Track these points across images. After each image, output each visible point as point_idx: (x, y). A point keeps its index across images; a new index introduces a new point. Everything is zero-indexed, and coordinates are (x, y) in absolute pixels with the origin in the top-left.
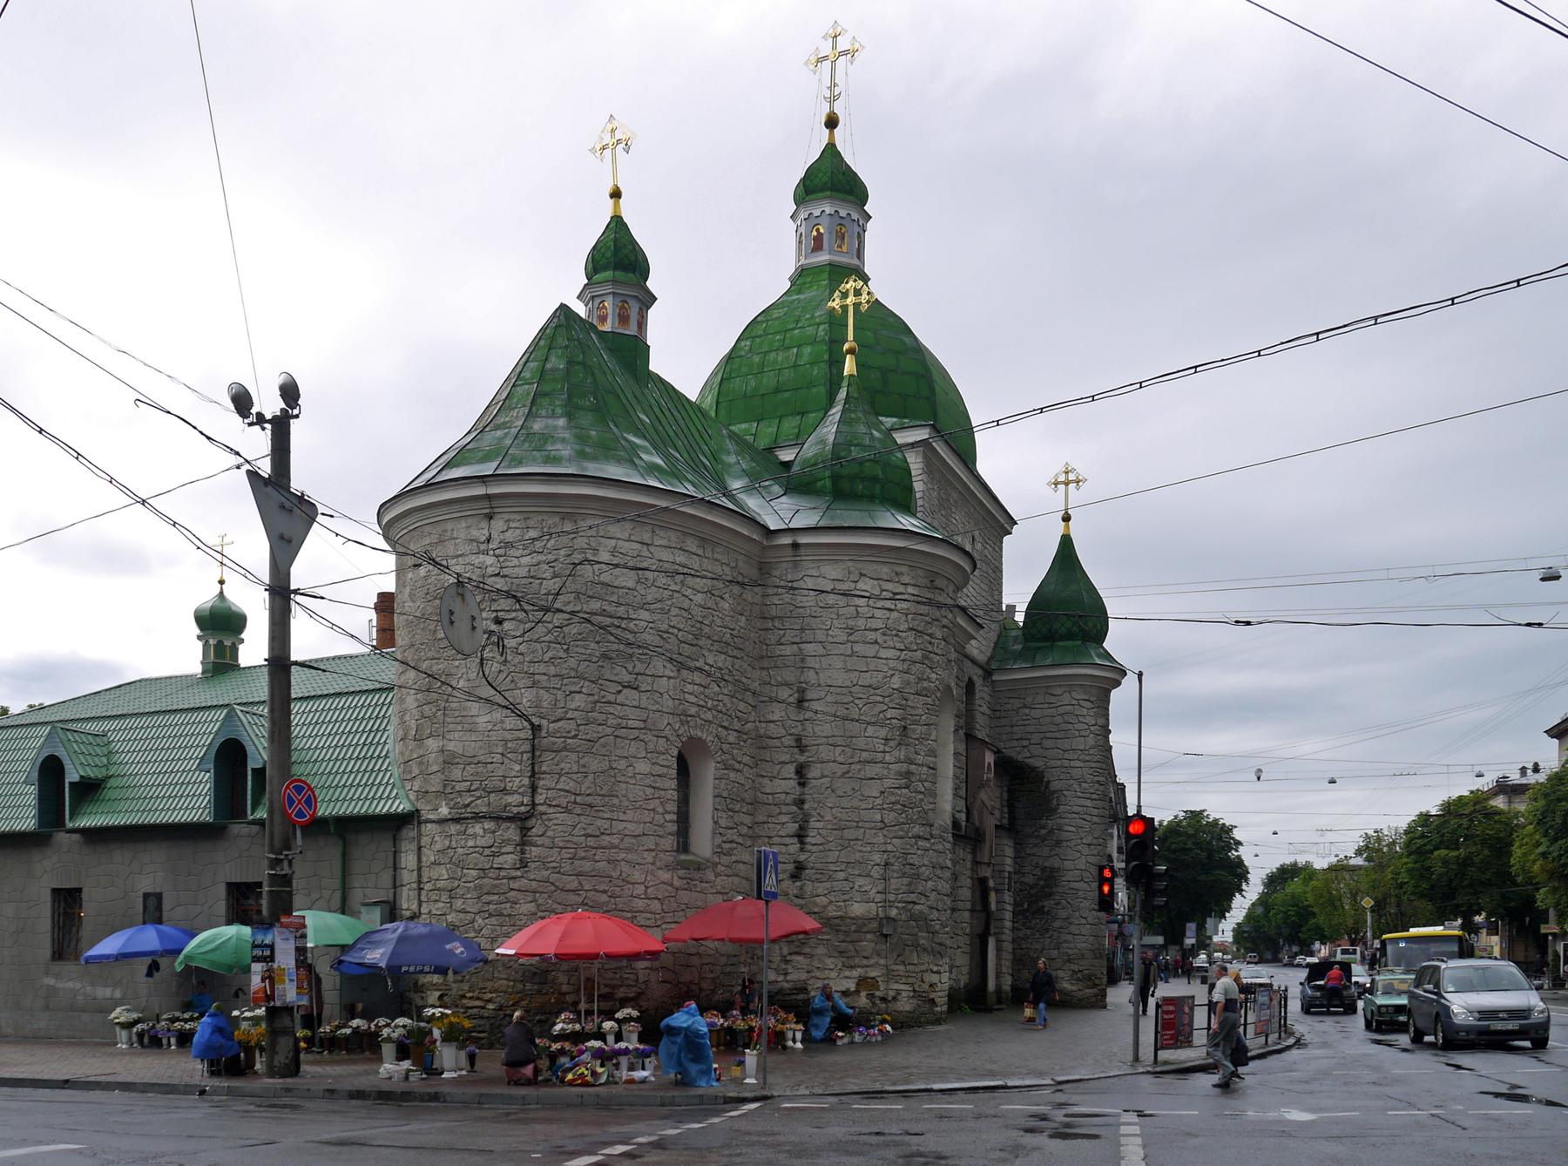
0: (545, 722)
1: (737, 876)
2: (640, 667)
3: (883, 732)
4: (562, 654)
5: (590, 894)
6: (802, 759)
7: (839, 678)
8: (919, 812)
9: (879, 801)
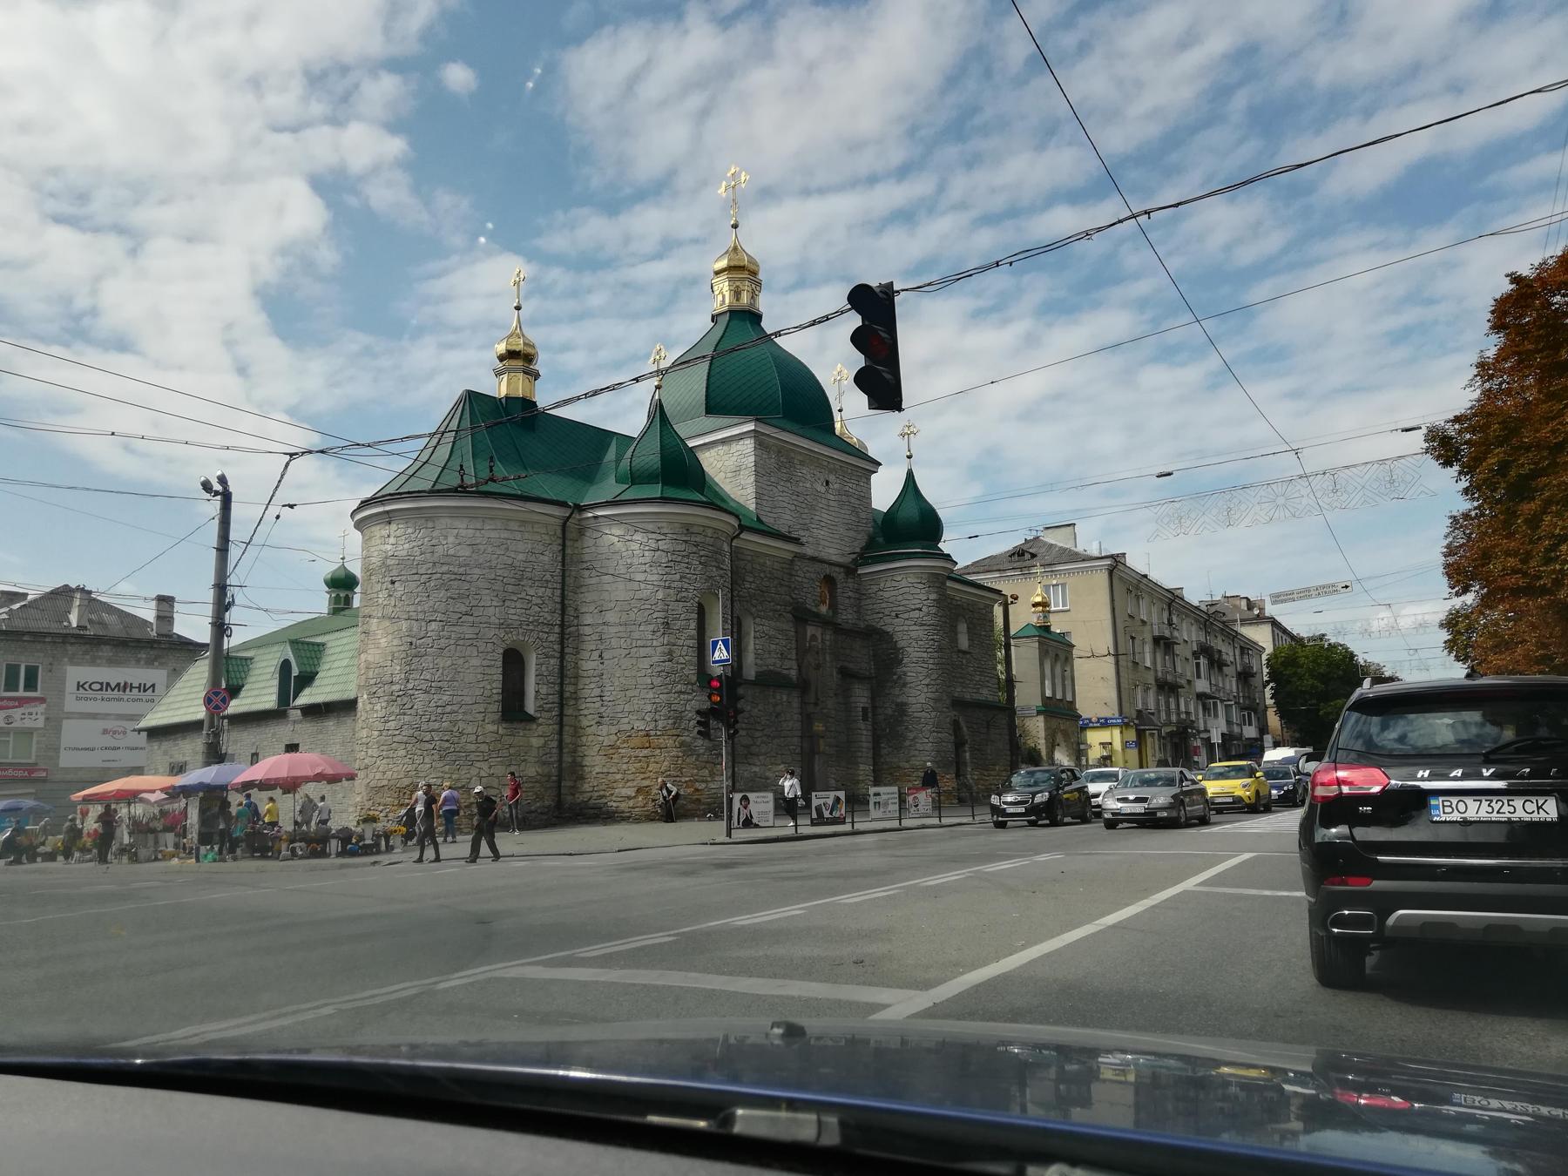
0: (414, 640)
2: (474, 603)
3: (651, 628)
4: (425, 599)
5: (438, 743)
6: (602, 647)
7: (622, 595)
9: (650, 671)
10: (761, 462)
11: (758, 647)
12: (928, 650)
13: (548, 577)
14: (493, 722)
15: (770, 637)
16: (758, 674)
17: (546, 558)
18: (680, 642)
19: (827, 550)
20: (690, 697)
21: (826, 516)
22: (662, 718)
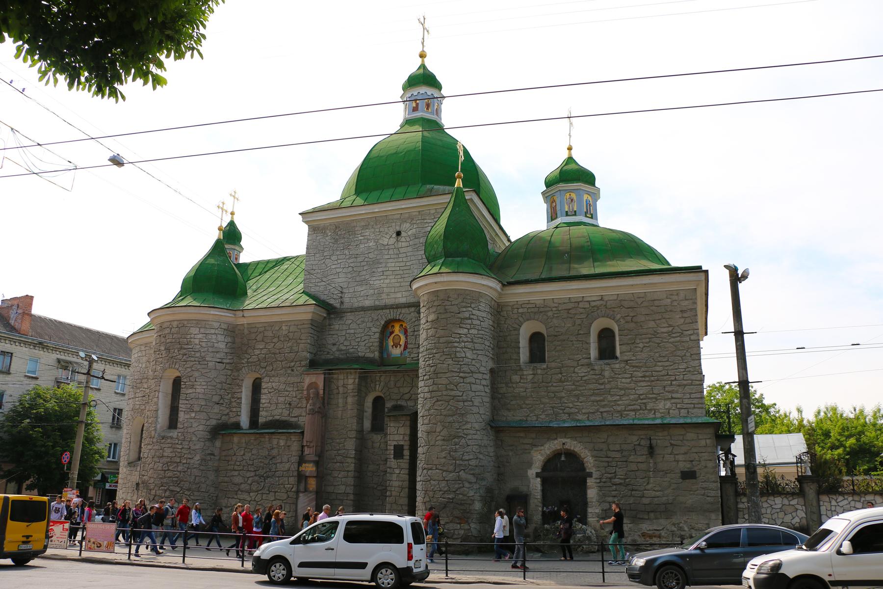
10: (314, 244)
15: (279, 391)
19: (392, 296)
21: (393, 264)
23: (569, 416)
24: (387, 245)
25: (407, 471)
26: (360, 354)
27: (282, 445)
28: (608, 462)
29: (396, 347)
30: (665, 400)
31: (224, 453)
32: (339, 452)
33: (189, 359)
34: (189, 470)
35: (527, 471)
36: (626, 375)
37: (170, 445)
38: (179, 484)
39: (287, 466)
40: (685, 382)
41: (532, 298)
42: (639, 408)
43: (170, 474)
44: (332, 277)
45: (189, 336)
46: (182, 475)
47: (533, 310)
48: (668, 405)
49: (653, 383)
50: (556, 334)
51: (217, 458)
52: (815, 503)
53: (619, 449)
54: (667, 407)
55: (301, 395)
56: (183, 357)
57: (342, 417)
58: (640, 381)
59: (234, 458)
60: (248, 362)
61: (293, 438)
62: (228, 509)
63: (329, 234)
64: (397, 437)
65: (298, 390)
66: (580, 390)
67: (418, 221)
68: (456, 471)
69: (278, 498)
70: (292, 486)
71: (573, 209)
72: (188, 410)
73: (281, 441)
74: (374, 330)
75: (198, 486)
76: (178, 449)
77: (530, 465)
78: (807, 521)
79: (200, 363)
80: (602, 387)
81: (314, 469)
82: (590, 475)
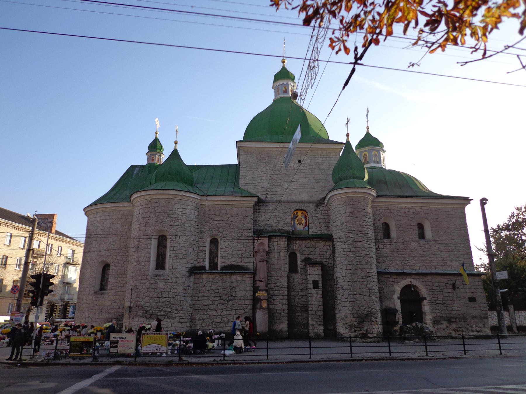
1: (118, 295)
8: (141, 272)
10: (246, 160)
11: (222, 253)
12: (346, 243)
13: (119, 232)
14: (91, 295)
16: (224, 268)
17: (118, 225)
18: (143, 255)
20: (145, 282)
21: (298, 178)
22: (134, 292)
23: (410, 267)
24: (293, 167)
25: (321, 296)
26: (280, 227)
27: (240, 280)
28: (433, 292)
29: (300, 225)
30: (455, 261)
31: (197, 285)
32: (277, 284)
33: (175, 224)
34: (177, 297)
35: (393, 296)
36: (436, 248)
37: (163, 280)
38: (170, 306)
39: (243, 293)
40: (464, 253)
41: (387, 205)
42: (443, 264)
43: (164, 300)
44: (259, 181)
45: (174, 209)
46: (172, 300)
47: (387, 211)
48: (457, 264)
49: (449, 253)
50: (399, 224)
51: (192, 288)
52: (513, 315)
53: (438, 285)
54: (457, 265)
55: (249, 250)
56: (170, 223)
57: (277, 263)
58: (443, 251)
59: (204, 288)
60: (209, 228)
61: (247, 276)
62: (201, 321)
63: (255, 156)
64: (314, 276)
65: (247, 247)
66: (414, 254)
67: (311, 156)
68: (371, 296)
69: (238, 313)
70: (247, 305)
71: (377, 160)
72: (175, 257)
73: (238, 278)
74: (288, 214)
75: (182, 307)
76: (169, 283)
77: (394, 292)
78: (511, 322)
79: (182, 227)
80: (425, 253)
81: (266, 294)
82: (425, 298)
